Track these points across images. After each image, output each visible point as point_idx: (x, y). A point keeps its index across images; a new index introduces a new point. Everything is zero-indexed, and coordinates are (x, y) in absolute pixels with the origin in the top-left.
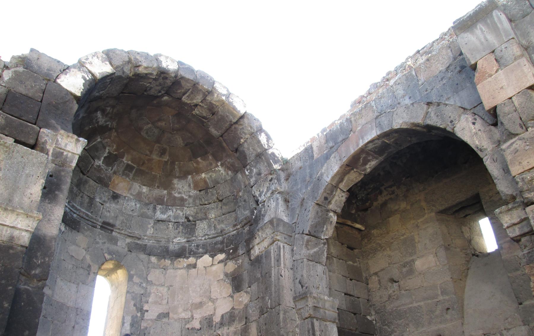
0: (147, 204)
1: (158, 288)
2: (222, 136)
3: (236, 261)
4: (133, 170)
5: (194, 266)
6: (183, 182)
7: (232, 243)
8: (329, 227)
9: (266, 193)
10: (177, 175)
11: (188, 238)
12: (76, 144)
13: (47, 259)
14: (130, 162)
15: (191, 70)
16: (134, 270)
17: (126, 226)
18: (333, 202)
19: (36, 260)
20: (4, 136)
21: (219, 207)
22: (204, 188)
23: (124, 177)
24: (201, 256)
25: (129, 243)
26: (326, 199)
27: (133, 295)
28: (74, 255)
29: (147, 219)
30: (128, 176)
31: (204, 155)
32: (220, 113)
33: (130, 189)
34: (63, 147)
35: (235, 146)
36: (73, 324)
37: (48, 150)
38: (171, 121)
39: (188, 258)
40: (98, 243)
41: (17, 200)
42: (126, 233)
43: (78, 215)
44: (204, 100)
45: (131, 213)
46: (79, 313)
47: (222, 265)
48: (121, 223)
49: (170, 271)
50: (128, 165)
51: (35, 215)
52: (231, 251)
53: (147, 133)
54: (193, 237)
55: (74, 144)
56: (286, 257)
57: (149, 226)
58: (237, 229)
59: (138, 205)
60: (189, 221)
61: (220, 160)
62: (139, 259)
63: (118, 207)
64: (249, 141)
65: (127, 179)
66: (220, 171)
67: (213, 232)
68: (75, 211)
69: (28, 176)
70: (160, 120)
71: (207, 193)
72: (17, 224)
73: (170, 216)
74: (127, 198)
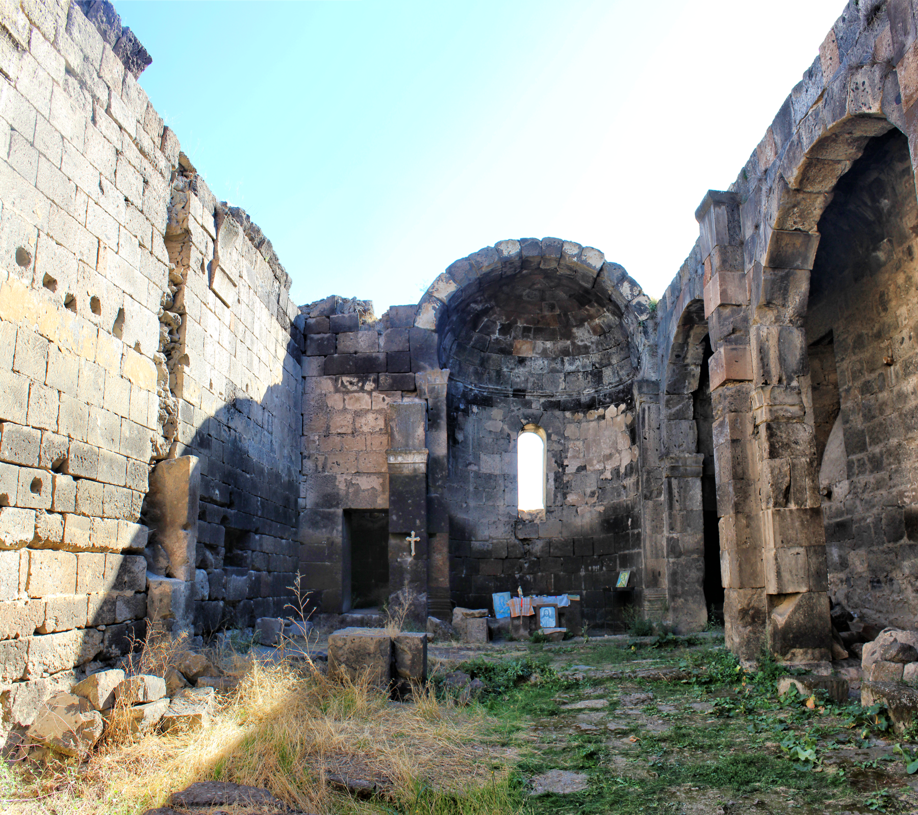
0: (554, 359)
5: (603, 417)
6: (582, 329)
8: (692, 381)
18: (689, 356)
22: (602, 332)
26: (678, 356)
30: (528, 337)
33: (534, 348)
39: (597, 409)
40: (513, 411)
47: (623, 415)
49: (584, 424)
57: (561, 380)
59: (546, 362)
62: (555, 417)
67: (617, 379)
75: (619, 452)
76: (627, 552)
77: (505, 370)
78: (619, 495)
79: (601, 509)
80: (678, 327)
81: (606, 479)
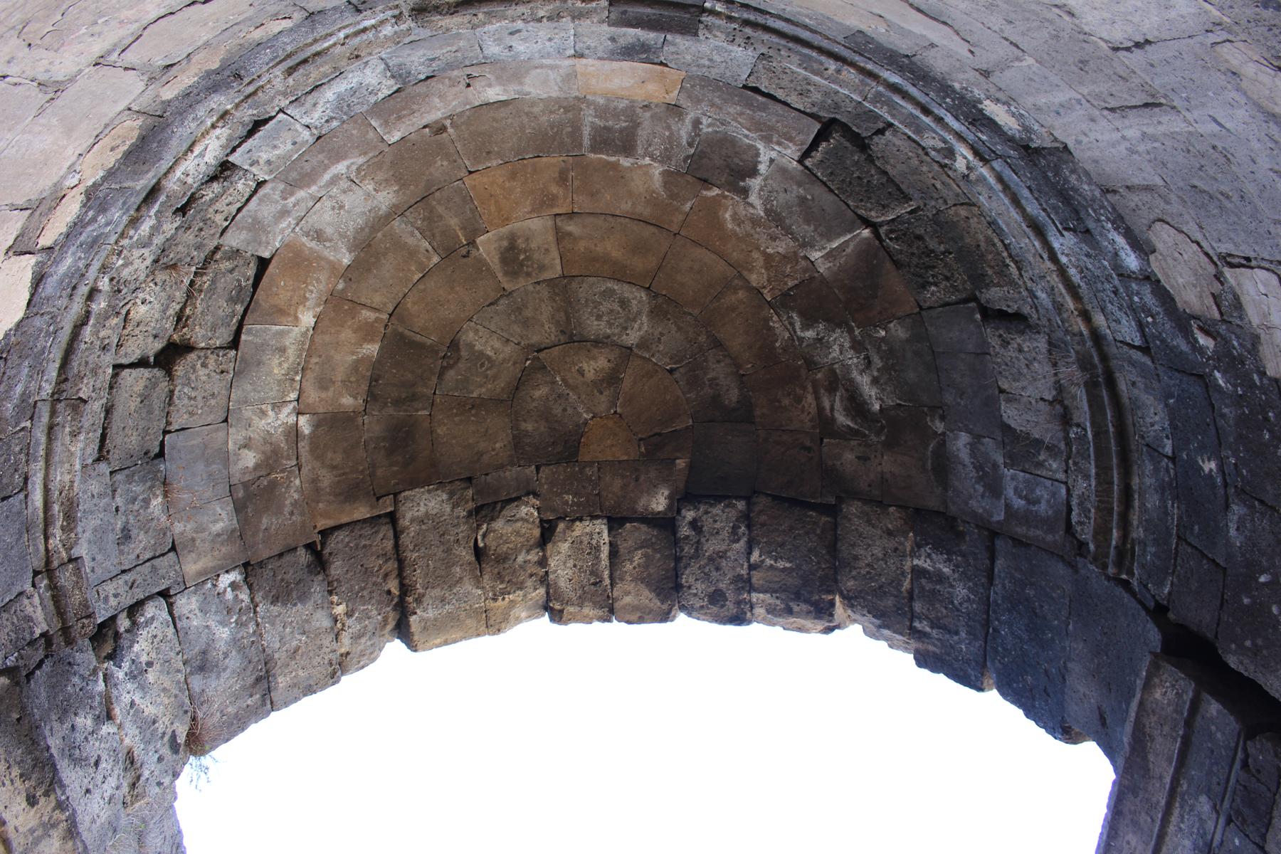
2: (392, 518)
4: (593, 139)
14: (625, 162)
23: (622, 105)
31: (374, 385)
32: (468, 586)
35: (337, 568)
38: (573, 397)
44: (544, 580)
53: (624, 303)
58: (48, 522)
61: (313, 437)
64: (327, 641)
65: (602, 101)
68: (897, 99)
70: (611, 379)
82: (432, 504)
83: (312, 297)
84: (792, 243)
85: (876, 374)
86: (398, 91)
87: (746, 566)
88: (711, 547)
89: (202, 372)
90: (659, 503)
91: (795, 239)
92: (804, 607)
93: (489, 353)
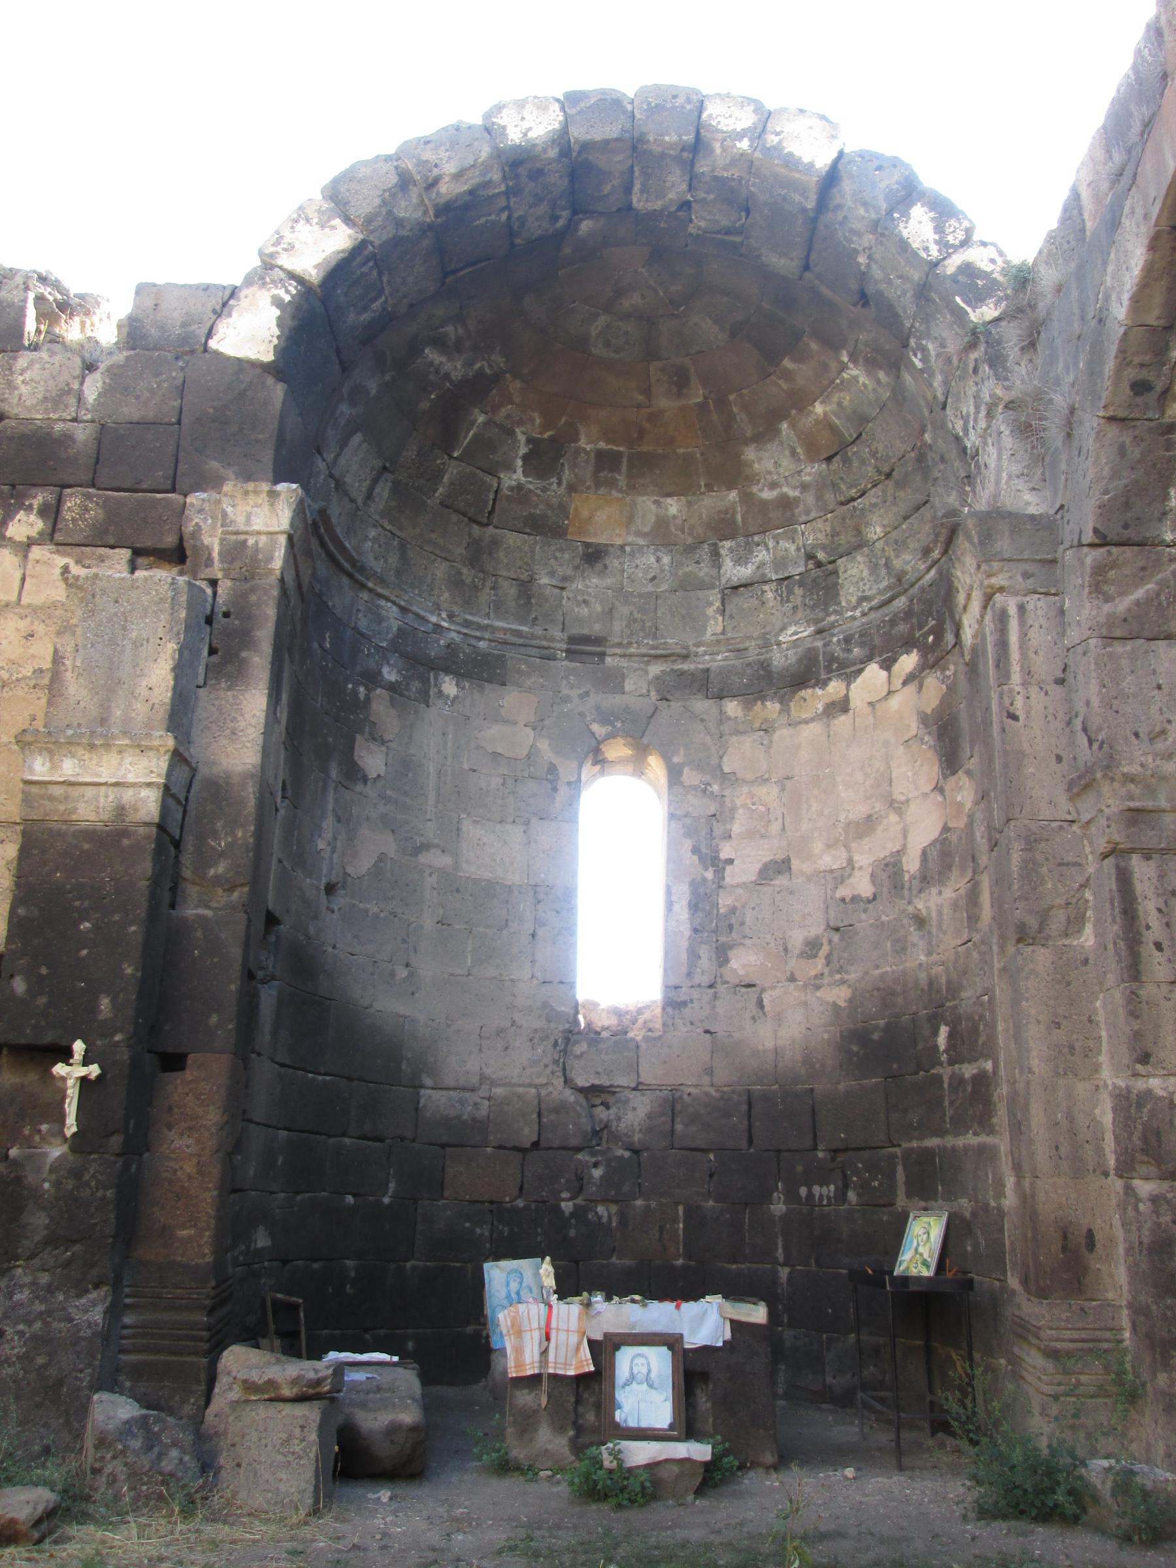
0: (690, 549)
1: (755, 789)
2: (807, 267)
3: (944, 669)
5: (842, 706)
6: (772, 447)
7: (930, 614)
9: (975, 420)
10: (749, 434)
11: (816, 621)
12: (272, 505)
13: (240, 834)
14: (602, 445)
15: (610, 103)
16: (682, 752)
17: (643, 629)
19: (215, 839)
20: (107, 550)
21: (890, 498)
22: (833, 448)
23: (602, 491)
24: (860, 671)
25: (657, 678)
26: (1140, 387)
27: (688, 821)
28: (499, 750)
29: (700, 594)
30: (612, 484)
33: (630, 521)
34: (242, 528)
35: (854, 285)
36: (529, 927)
37: (207, 547)
39: (824, 684)
40: (567, 699)
41: (119, 713)
42: (644, 650)
43: (490, 640)
44: (693, 181)
45: (650, 588)
46: (541, 896)
48: (628, 626)
49: (782, 734)
50: (600, 454)
51: (157, 743)
52: (931, 638)
53: (608, 345)
54: (829, 615)
55: (266, 507)
56: (1034, 643)
57: (710, 611)
58: (935, 563)
59: (666, 560)
60: (819, 565)
63: (609, 581)
65: (614, 493)
66: (855, 379)
68: (478, 634)
69: (137, 644)
71: (846, 461)
72: (124, 776)
73: (762, 565)
74: (628, 549)
75: (897, 807)
76: (933, 1142)
77: (545, 580)
78: (901, 947)
79: (840, 995)
80: (1152, 247)
81: (855, 899)
82: (775, 260)
83: (811, 419)
84: (497, 418)
85: (432, 369)
86: (721, 540)
87: (512, 204)
88: (543, 209)
89: (880, 449)
90: (586, 226)
91: (495, 423)
92: (459, 202)
93: (710, 322)
